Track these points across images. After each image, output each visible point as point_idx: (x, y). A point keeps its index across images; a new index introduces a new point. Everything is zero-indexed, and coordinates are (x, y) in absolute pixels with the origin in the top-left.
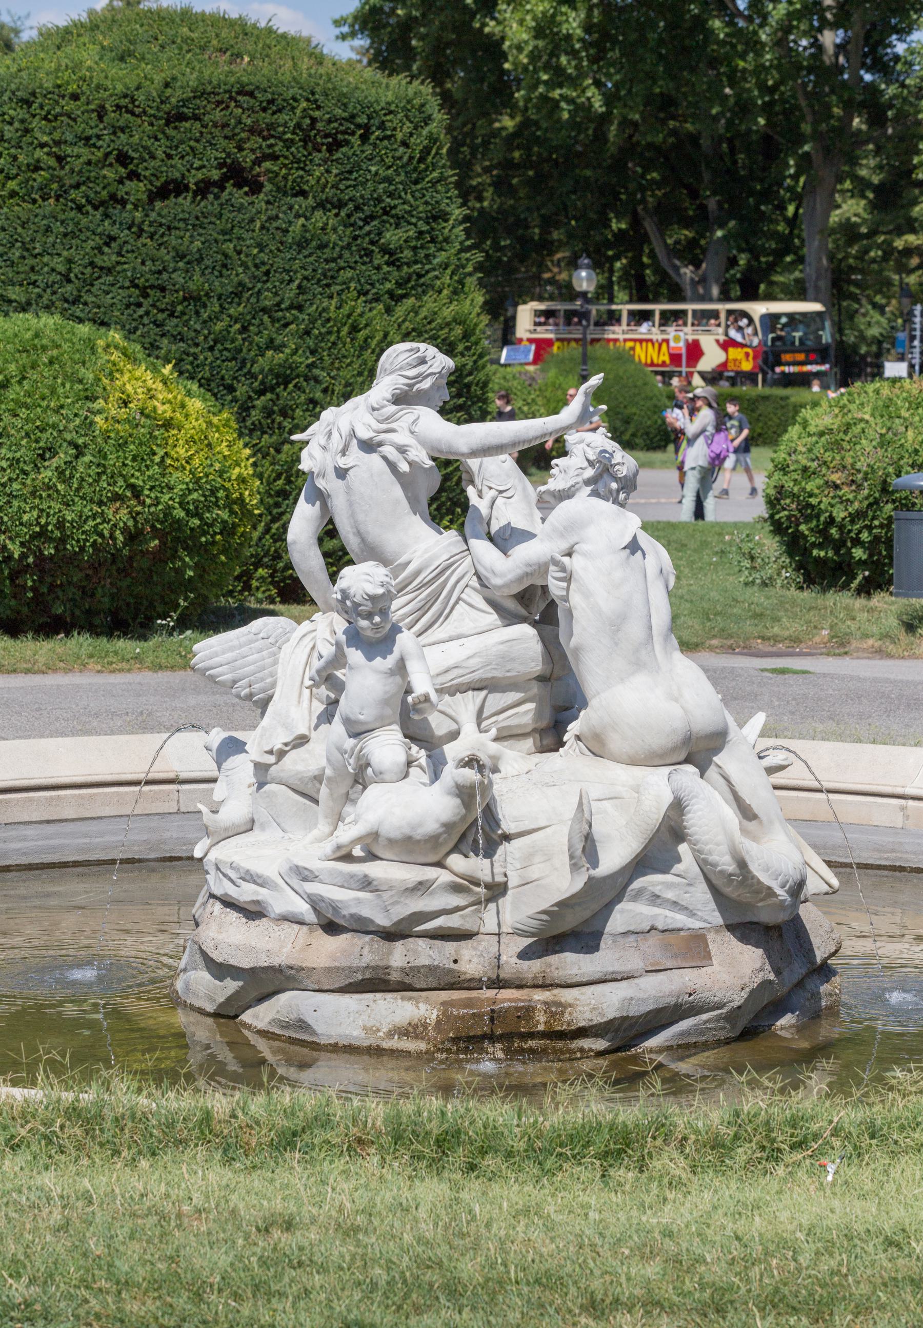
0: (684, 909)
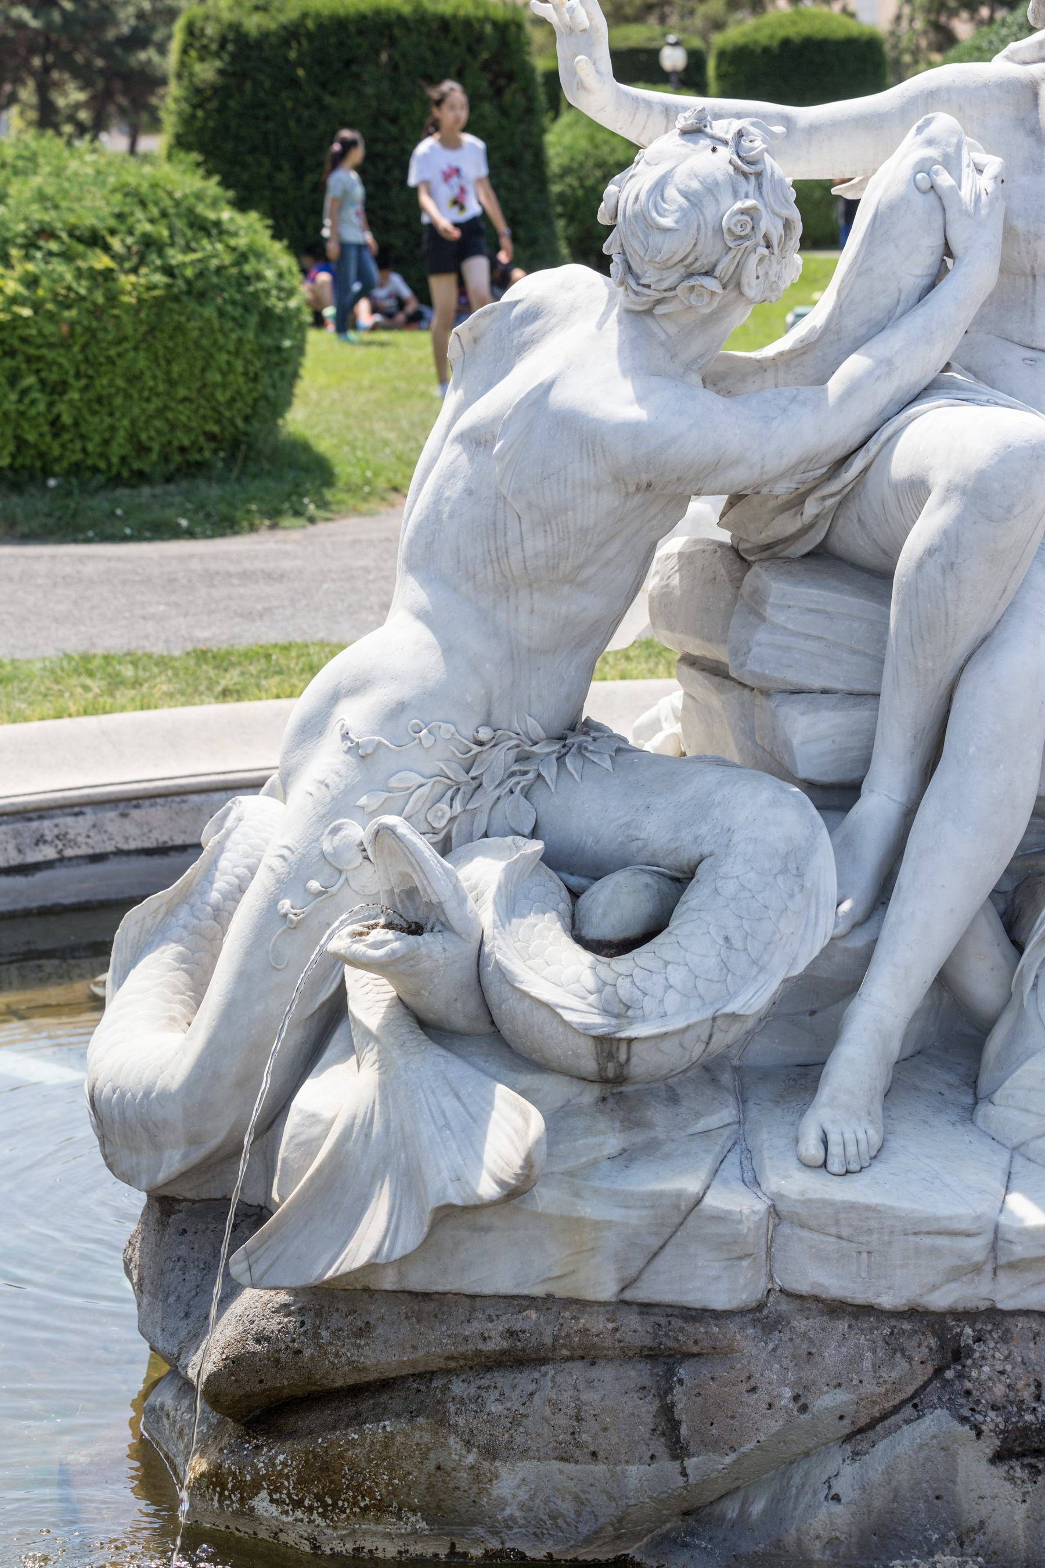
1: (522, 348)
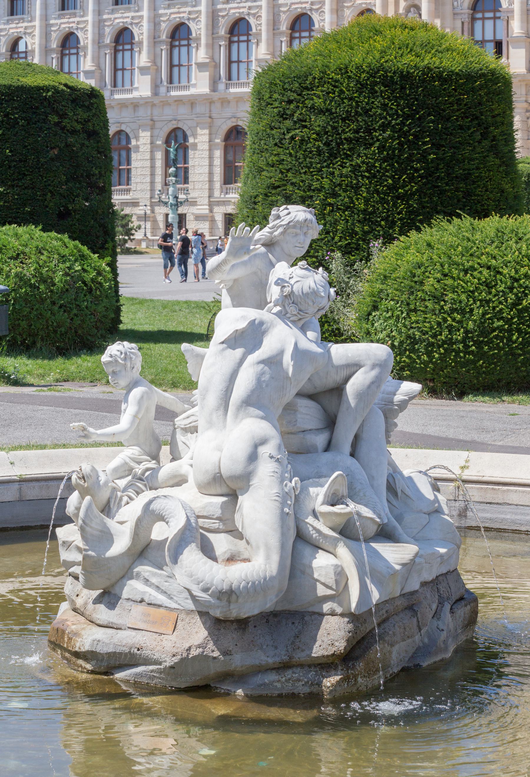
0: (164, 592)
1: (264, 333)
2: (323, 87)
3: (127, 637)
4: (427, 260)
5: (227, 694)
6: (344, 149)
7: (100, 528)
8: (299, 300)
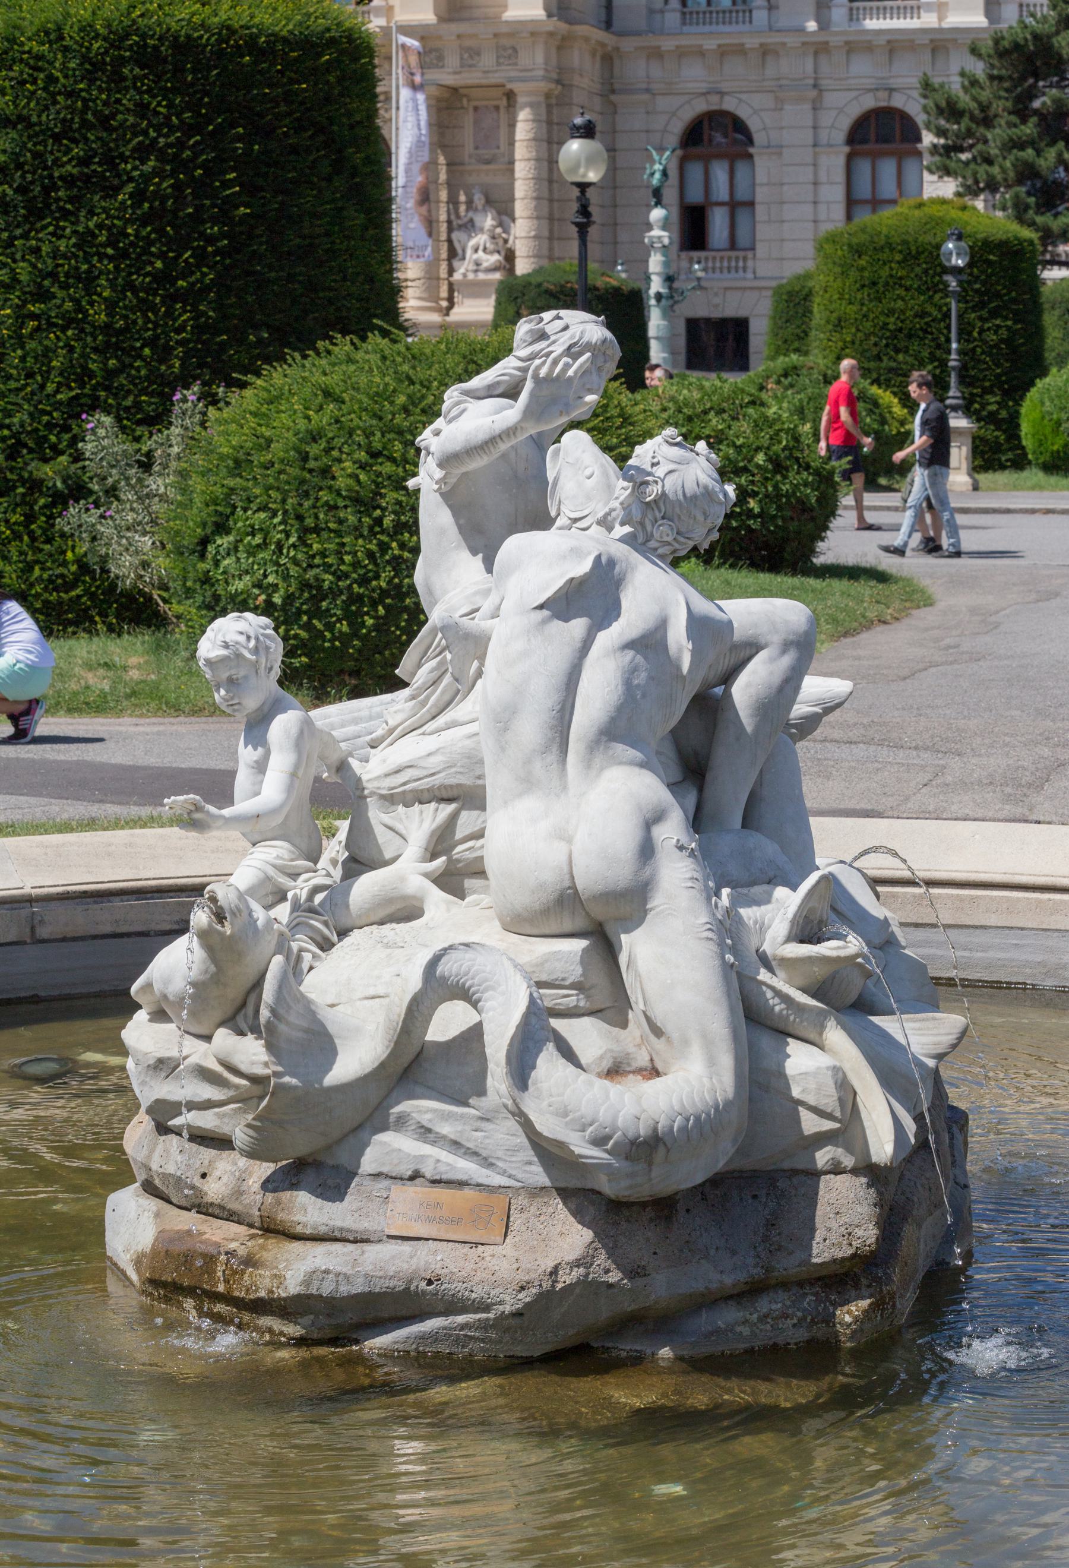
0: (472, 1154)
2: (11, 69)
3: (393, 1257)
4: (330, 424)
5: (637, 1360)
6: (59, 199)
7: (304, 1024)
8: (677, 510)
